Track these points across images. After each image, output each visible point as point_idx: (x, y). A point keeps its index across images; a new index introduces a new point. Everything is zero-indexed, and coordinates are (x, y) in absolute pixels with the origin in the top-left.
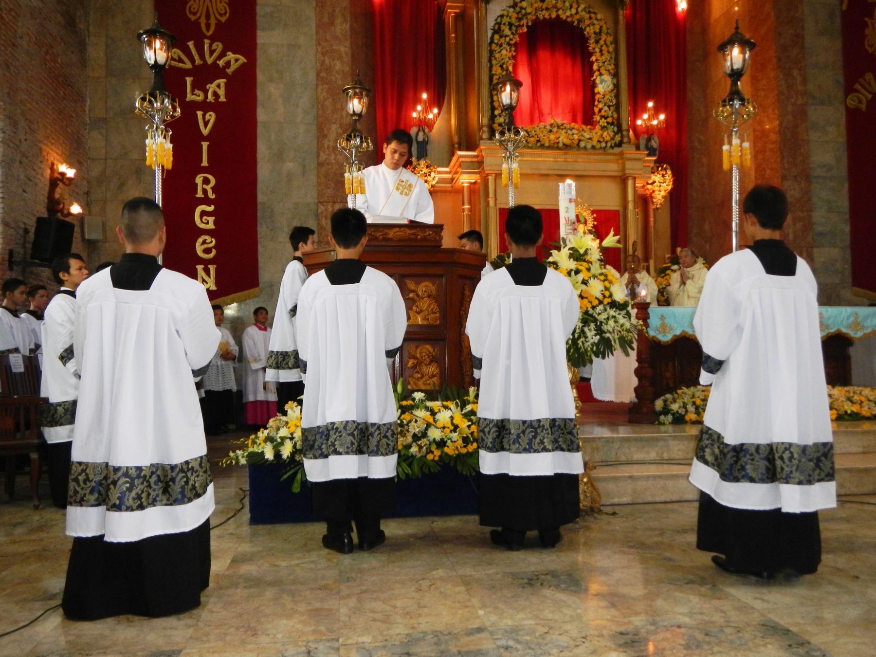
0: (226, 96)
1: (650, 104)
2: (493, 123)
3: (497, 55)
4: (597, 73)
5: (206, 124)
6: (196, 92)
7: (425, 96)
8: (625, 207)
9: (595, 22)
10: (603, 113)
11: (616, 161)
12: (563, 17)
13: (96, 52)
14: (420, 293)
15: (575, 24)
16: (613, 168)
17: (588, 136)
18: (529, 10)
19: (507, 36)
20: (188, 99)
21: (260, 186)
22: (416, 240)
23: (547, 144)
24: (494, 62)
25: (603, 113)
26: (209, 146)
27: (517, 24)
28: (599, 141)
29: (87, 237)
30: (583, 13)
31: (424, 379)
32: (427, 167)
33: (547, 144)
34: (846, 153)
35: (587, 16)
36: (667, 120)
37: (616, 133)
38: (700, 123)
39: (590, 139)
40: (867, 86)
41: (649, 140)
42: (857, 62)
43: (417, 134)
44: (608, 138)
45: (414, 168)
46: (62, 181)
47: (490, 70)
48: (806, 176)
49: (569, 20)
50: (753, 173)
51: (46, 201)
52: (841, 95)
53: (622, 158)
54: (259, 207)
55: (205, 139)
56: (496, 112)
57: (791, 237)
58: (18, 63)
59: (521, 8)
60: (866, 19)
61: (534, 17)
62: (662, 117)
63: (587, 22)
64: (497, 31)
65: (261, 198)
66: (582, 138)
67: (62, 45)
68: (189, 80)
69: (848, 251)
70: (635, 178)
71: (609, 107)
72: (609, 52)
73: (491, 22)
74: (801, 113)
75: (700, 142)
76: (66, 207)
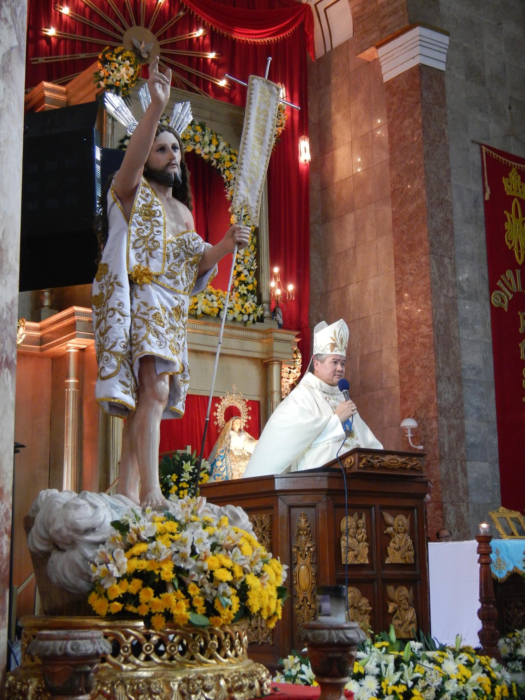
11: (260, 340)
12: (198, 152)
14: (396, 527)
16: (255, 348)
22: (405, 469)
25: (242, 277)
28: (241, 313)
30: (224, 153)
31: (405, 626)
34: (492, 355)
35: (229, 157)
38: (319, 298)
39: (231, 309)
40: (507, 283)
42: (498, 258)
44: (250, 310)
48: (458, 379)
49: (206, 157)
50: (395, 367)
52: (486, 291)
57: (446, 449)
60: (505, 212)
66: (221, 306)
69: (497, 466)
70: (281, 364)
71: (249, 271)
74: (452, 307)
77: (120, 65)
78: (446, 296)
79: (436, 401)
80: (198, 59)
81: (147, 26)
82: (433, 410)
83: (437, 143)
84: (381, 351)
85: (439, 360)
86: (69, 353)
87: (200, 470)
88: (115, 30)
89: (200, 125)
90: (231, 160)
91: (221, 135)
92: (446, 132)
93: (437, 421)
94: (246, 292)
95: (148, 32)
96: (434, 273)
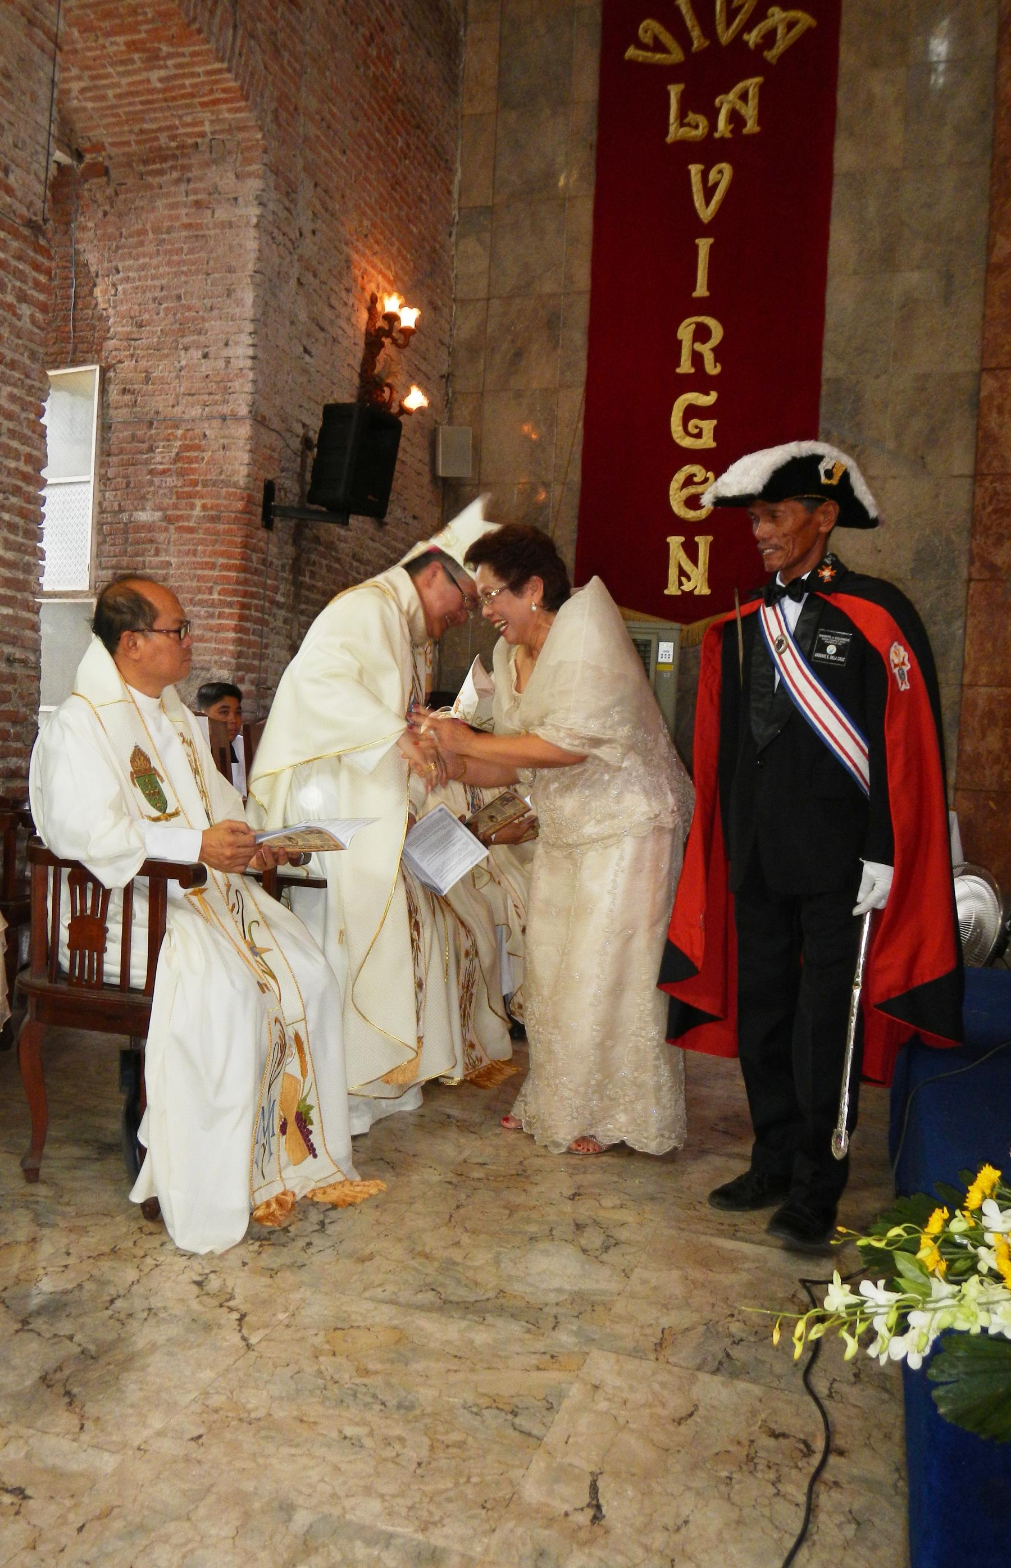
0: (760, 121)
5: (709, 193)
6: (692, 117)
13: (478, 58)
20: (670, 139)
21: (831, 337)
26: (712, 248)
29: (441, 473)
46: (388, 334)
51: (356, 381)
54: (825, 389)
55: (704, 230)
58: (299, 48)
65: (830, 367)
67: (406, 30)
68: (675, 91)
76: (395, 395)
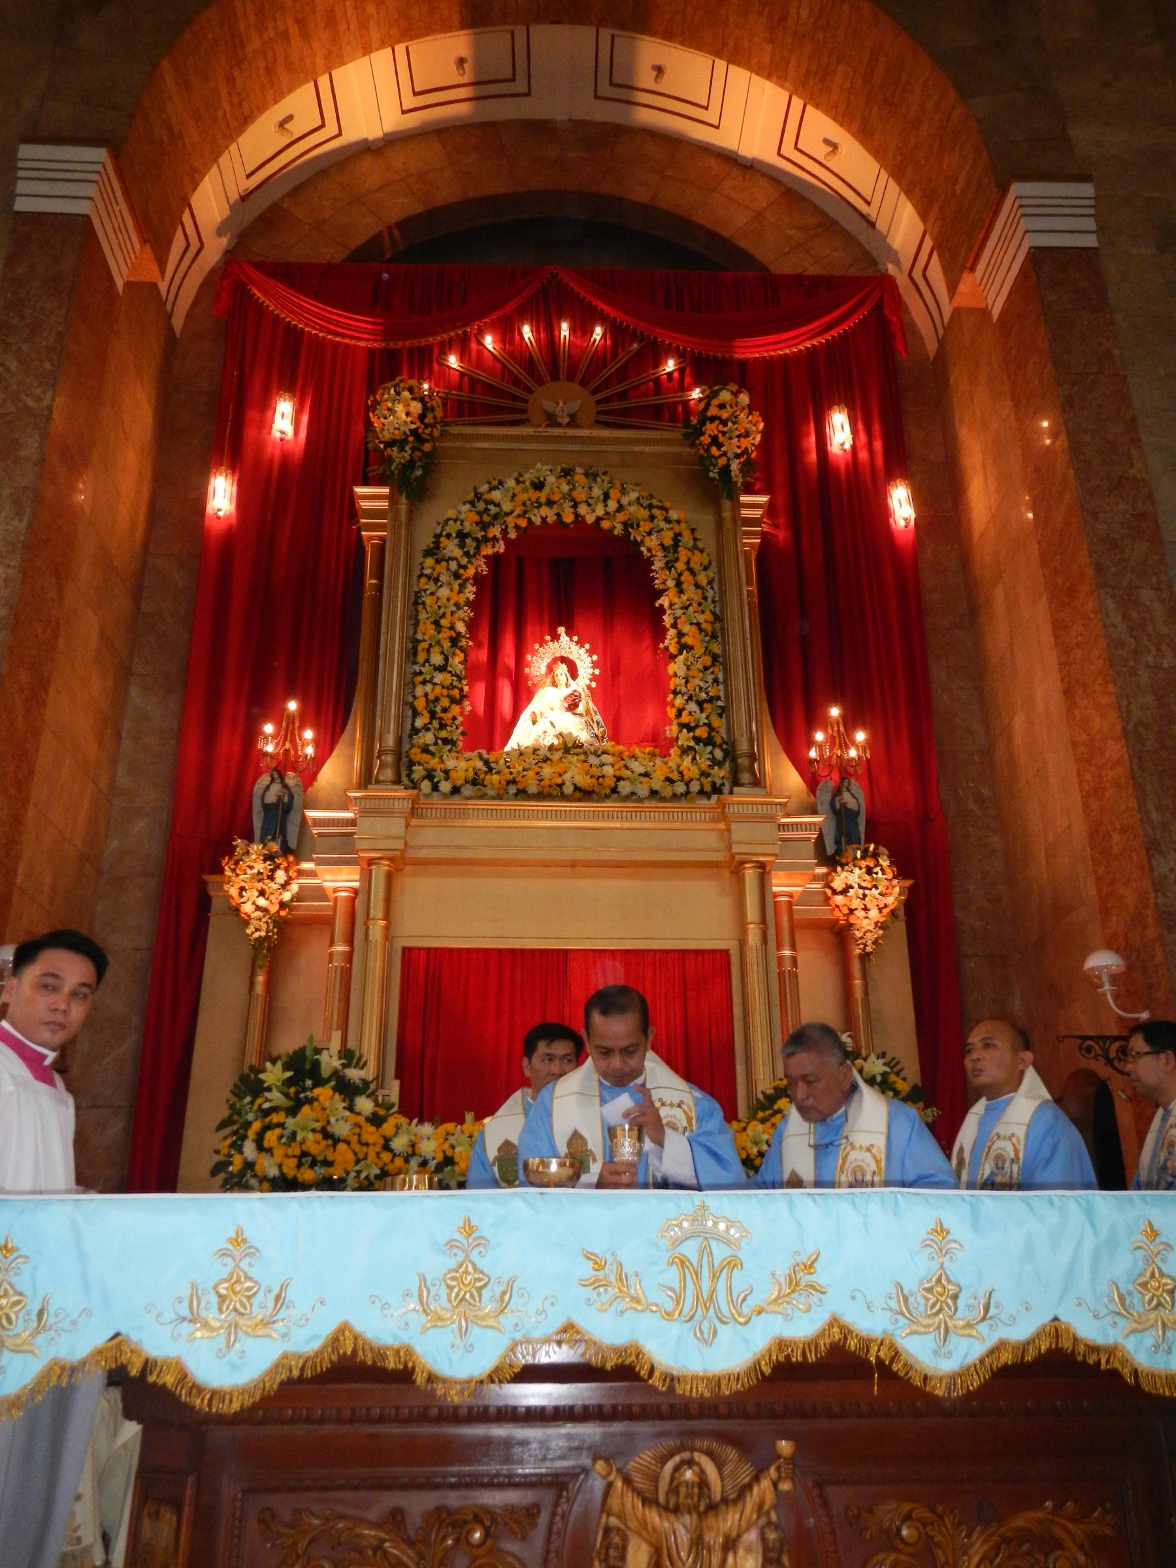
1: (835, 712)
2: (413, 746)
3: (429, 600)
4: (672, 633)
7: (292, 706)
8: (742, 943)
9: (662, 524)
10: (685, 718)
15: (618, 530)
17: (642, 770)
18: (507, 507)
19: (452, 559)
23: (533, 789)
24: (423, 615)
27: (479, 535)
32: (269, 858)
33: (533, 789)
36: (870, 744)
37: (715, 762)
39: (646, 775)
41: (837, 792)
43: (267, 788)
44: (694, 772)
45: (237, 863)
47: (416, 632)
49: (605, 525)
50: (1088, 852)
53: (724, 817)
56: (419, 723)
59: (487, 502)
61: (523, 523)
62: (861, 736)
63: (646, 526)
64: (433, 551)
66: (627, 773)
71: (700, 704)
72: (697, 586)
73: (427, 541)
75: (980, 800)
77: (394, 401)
78: (1158, 667)
79: (1152, 900)
80: (675, 404)
81: (570, 378)
82: (1150, 921)
83: (1091, 378)
84: (1070, 825)
85: (1150, 806)
86: (336, 898)
87: (319, 1082)
88: (515, 398)
89: (586, 475)
90: (652, 518)
91: (637, 484)
92: (1116, 352)
93: (1163, 946)
94: (692, 744)
95: (575, 386)
96: (1114, 625)
